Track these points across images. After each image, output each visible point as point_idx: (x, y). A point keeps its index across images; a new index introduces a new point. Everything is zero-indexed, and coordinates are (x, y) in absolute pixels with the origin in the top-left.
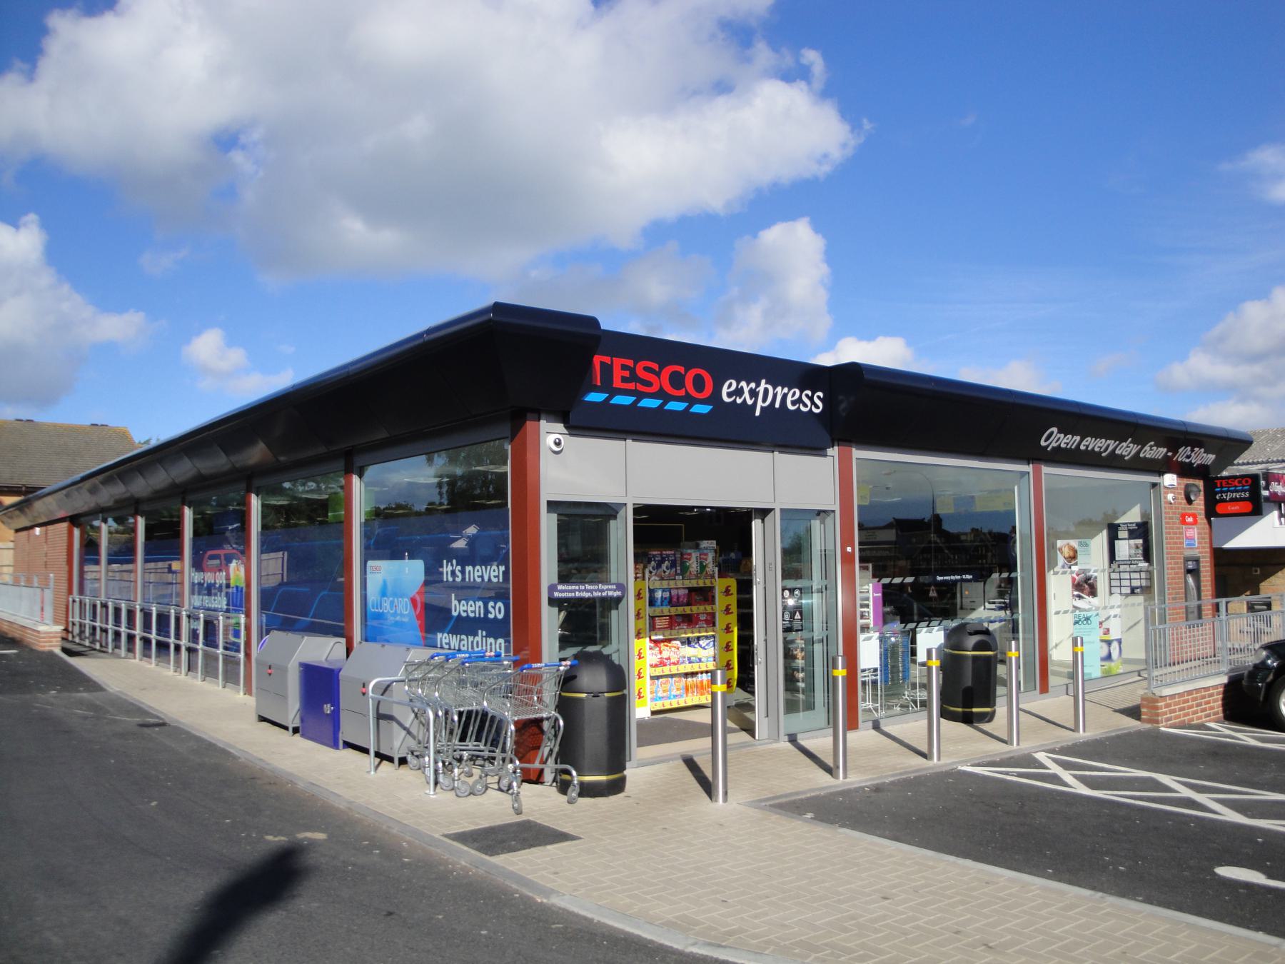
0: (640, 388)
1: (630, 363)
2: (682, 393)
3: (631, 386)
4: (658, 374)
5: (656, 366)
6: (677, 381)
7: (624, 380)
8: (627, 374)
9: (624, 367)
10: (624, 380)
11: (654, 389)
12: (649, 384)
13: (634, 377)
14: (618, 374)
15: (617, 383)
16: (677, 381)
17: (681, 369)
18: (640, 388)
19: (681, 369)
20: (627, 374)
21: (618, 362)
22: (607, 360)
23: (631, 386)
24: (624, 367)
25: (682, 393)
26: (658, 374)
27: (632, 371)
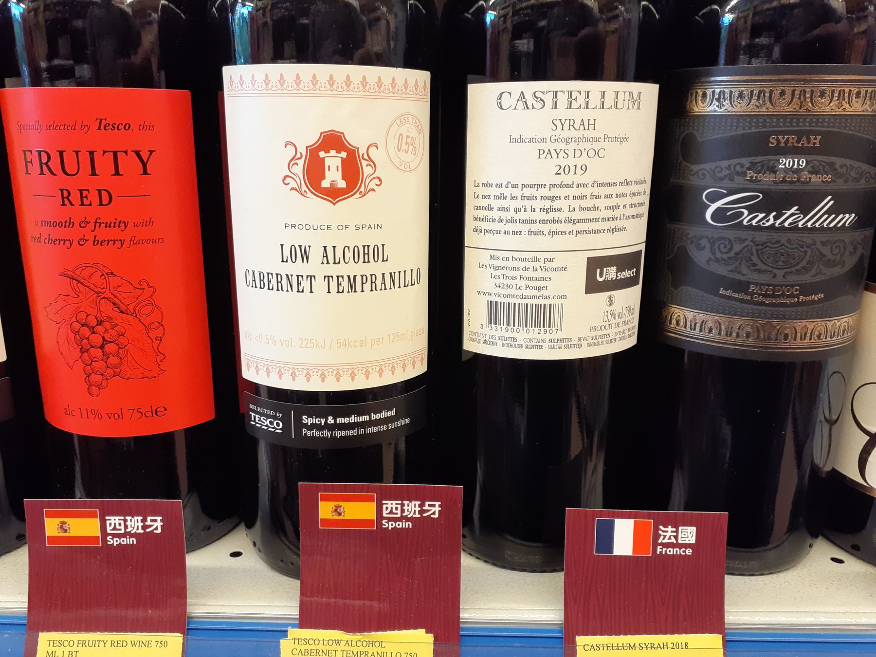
0: (262, 423)
1: (260, 417)
2: (273, 426)
3: (260, 422)
4: (266, 420)
5: (266, 419)
6: (271, 423)
7: (258, 420)
9: (258, 417)
10: (258, 420)
11: (265, 424)
12: (264, 423)
13: (260, 420)
14: (257, 419)
17: (273, 420)
18: (262, 423)
19: (273, 420)
21: (257, 416)
22: (255, 415)
23: (260, 422)
24: (258, 417)
25: (273, 426)
27: (260, 418)
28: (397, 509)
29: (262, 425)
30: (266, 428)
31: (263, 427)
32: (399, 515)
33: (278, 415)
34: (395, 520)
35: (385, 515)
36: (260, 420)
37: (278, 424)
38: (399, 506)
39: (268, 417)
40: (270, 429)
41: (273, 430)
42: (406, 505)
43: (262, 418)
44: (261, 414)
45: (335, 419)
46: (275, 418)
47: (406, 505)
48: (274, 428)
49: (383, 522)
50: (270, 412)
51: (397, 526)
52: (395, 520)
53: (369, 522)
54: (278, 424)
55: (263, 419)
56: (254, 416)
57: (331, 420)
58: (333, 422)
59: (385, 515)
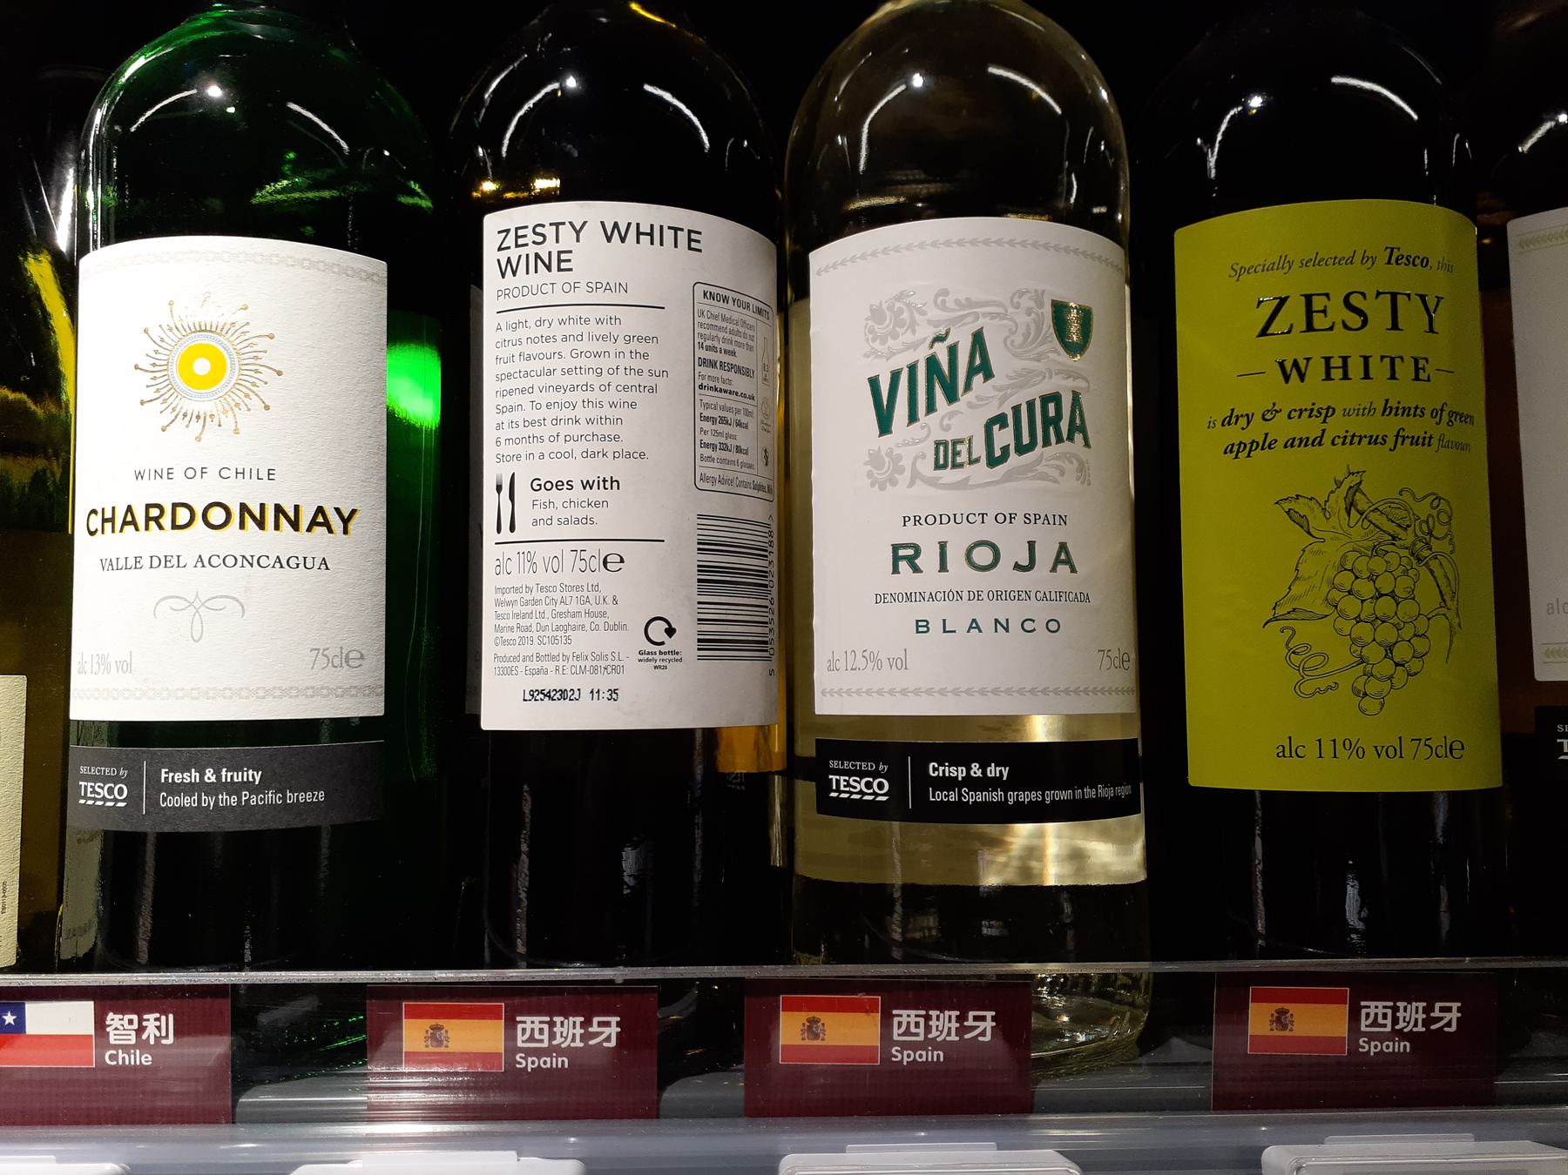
0: (852, 790)
1: (847, 778)
2: (871, 791)
3: (847, 789)
4: (859, 783)
5: (858, 779)
6: (869, 785)
7: (845, 786)
8: (845, 783)
9: (845, 780)
10: (845, 786)
12: (855, 788)
13: (848, 785)
14: (843, 783)
15: (842, 788)
16: (869, 785)
17: (871, 780)
18: (852, 790)
19: (871, 780)
20: (845, 783)
21: (842, 778)
22: (838, 777)
23: (847, 789)
24: (845, 780)
25: (871, 791)
26: (859, 783)
27: (848, 782)
29: (852, 793)
30: (858, 797)
31: (854, 797)
33: (881, 767)
36: (848, 785)
37: (881, 786)
39: (862, 774)
40: (866, 798)
41: (871, 798)
44: (849, 773)
45: (983, 767)
46: (875, 775)
48: (874, 793)
50: (867, 766)
54: (881, 786)
55: (854, 781)
56: (836, 779)
57: (976, 770)
58: (979, 774)
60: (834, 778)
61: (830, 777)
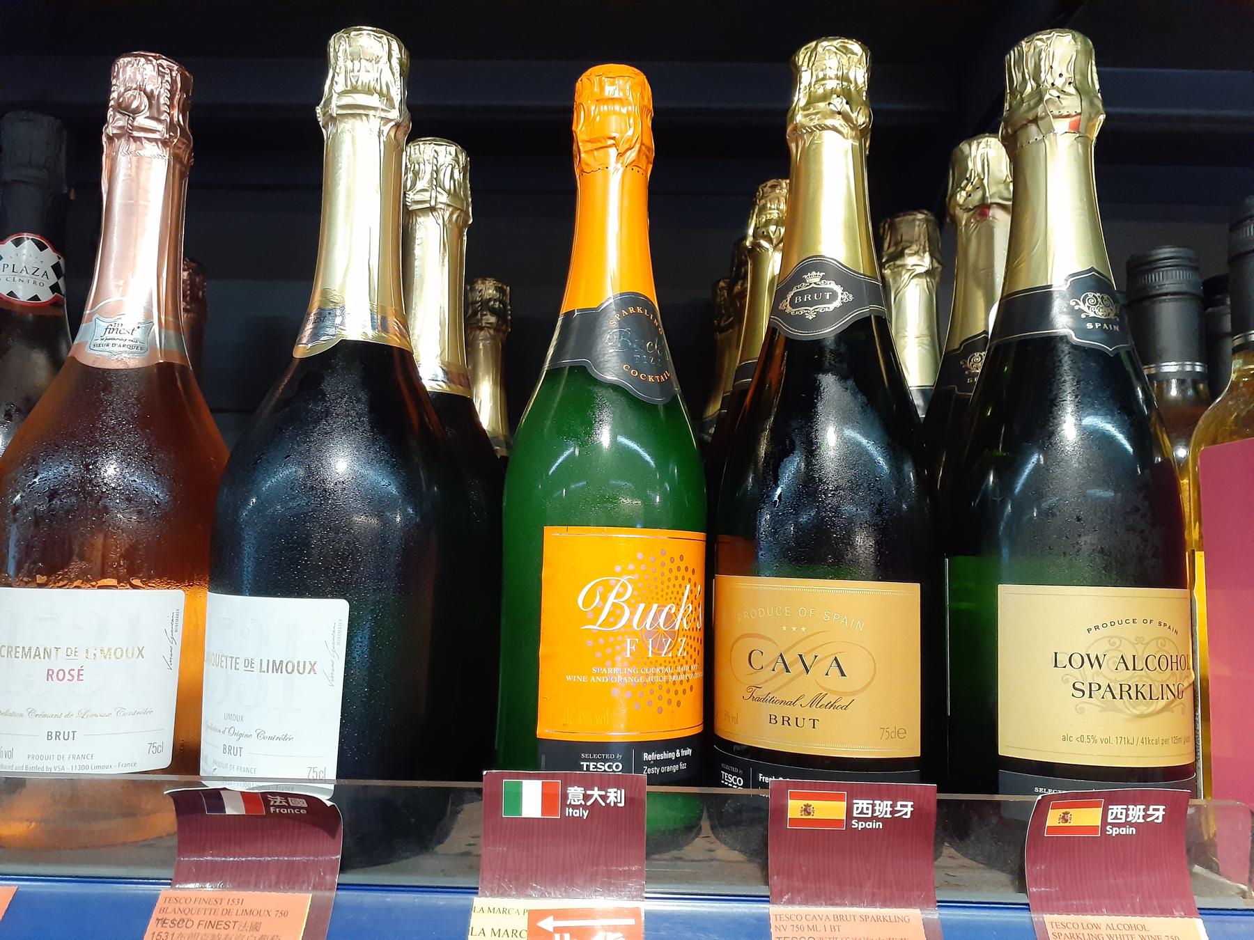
1: (595, 764)
3: (595, 770)
13: (596, 767)
14: (591, 767)
15: (591, 769)
18: (599, 770)
21: (592, 764)
22: (588, 763)
27: (596, 766)
28: (867, 809)
32: (870, 816)
34: (866, 820)
35: (855, 815)
38: (870, 806)
42: (878, 805)
43: (599, 764)
44: (597, 761)
47: (878, 805)
49: (853, 822)
51: (864, 823)
52: (866, 820)
53: (837, 822)
59: (855, 815)
60: (585, 764)
61: (582, 763)
